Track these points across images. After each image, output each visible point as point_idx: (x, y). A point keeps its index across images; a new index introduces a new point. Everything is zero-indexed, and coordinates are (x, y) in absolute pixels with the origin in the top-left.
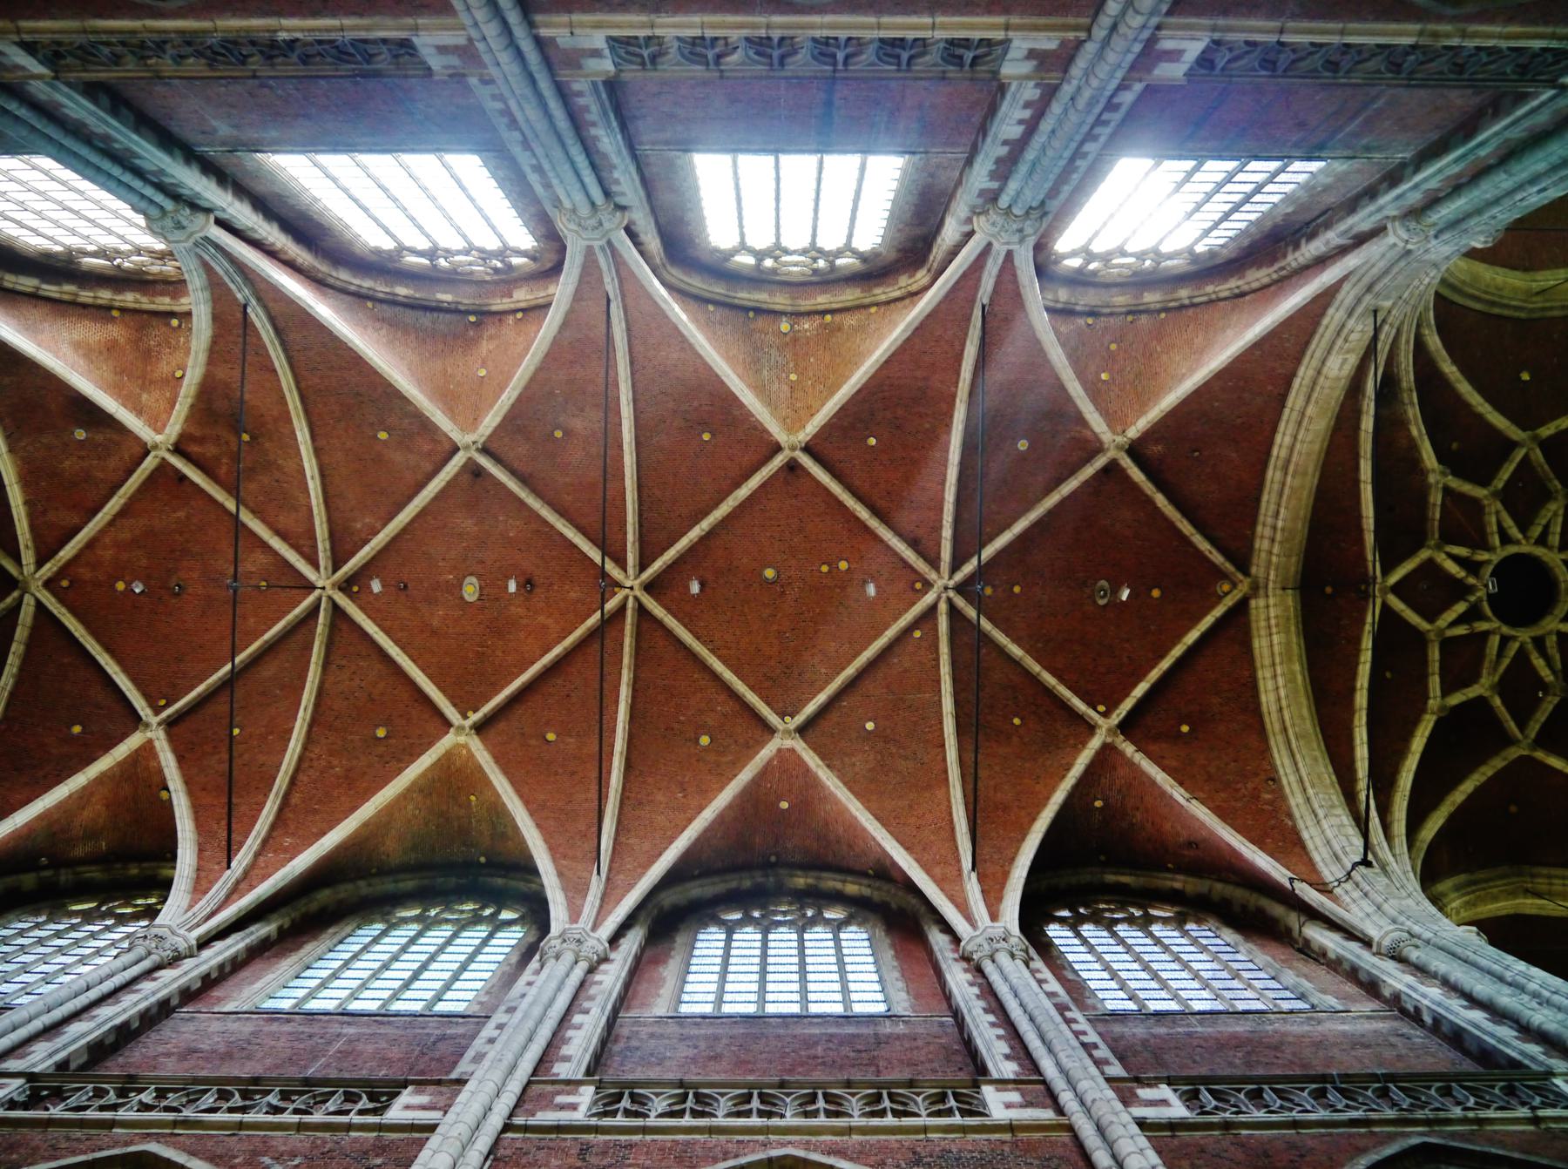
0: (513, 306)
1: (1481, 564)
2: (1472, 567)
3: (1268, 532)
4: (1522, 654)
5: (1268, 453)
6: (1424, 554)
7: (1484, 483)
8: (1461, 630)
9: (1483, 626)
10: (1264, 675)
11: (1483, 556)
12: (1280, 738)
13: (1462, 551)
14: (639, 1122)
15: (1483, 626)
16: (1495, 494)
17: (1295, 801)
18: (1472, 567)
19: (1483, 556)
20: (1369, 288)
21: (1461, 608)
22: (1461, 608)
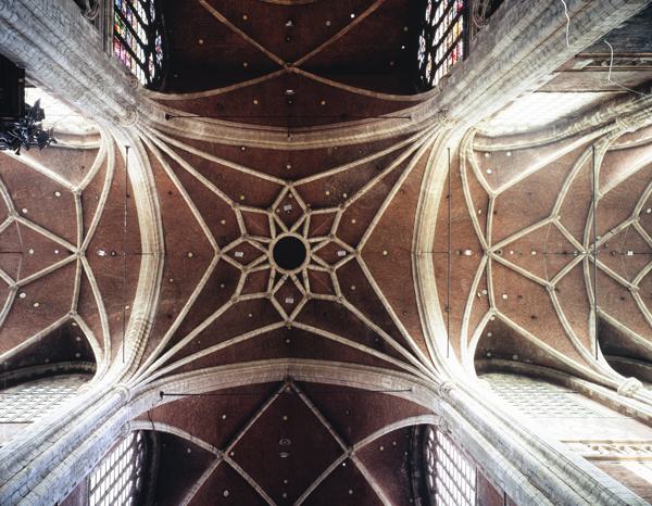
1: (277, 273)
4: (317, 253)
7: (239, 272)
9: (305, 273)
11: (273, 274)
13: (271, 283)
15: (305, 273)
16: (245, 270)
18: (278, 276)
19: (273, 274)
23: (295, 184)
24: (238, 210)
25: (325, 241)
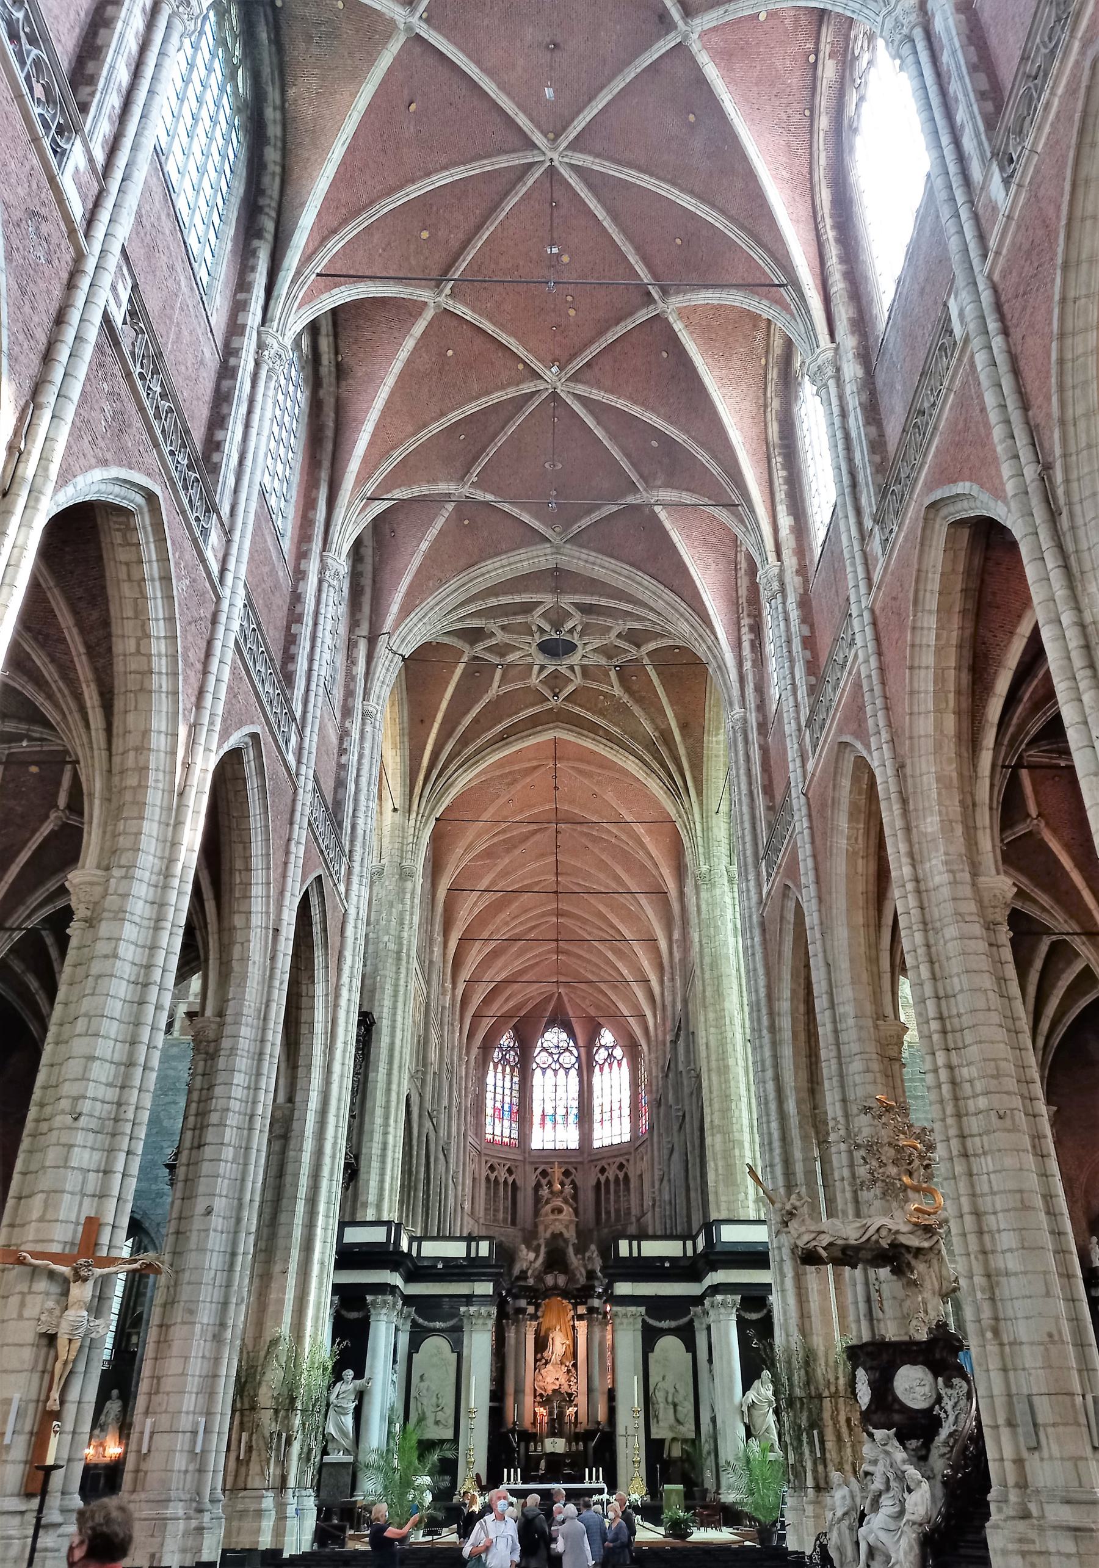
0: (821, 55)
2: (571, 631)
3: (592, 559)
5: (639, 569)
6: (577, 615)
8: (534, 628)
9: (537, 636)
10: (504, 559)
11: (576, 636)
12: (466, 579)
13: (579, 628)
14: (161, 439)
17: (431, 601)
19: (576, 636)
20: (719, 667)
21: (547, 627)
22: (547, 627)
23: (547, 706)
24: (618, 691)
25: (511, 658)
